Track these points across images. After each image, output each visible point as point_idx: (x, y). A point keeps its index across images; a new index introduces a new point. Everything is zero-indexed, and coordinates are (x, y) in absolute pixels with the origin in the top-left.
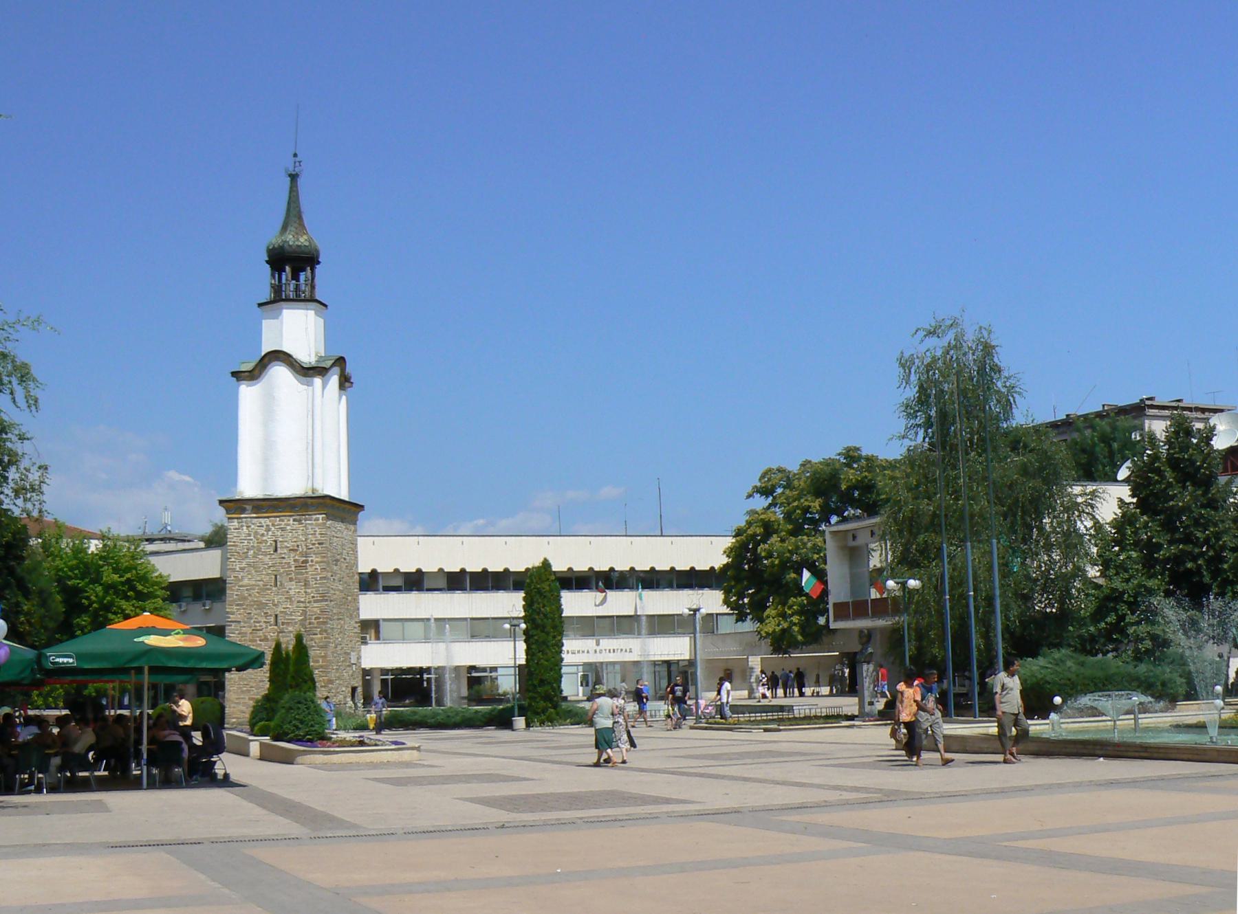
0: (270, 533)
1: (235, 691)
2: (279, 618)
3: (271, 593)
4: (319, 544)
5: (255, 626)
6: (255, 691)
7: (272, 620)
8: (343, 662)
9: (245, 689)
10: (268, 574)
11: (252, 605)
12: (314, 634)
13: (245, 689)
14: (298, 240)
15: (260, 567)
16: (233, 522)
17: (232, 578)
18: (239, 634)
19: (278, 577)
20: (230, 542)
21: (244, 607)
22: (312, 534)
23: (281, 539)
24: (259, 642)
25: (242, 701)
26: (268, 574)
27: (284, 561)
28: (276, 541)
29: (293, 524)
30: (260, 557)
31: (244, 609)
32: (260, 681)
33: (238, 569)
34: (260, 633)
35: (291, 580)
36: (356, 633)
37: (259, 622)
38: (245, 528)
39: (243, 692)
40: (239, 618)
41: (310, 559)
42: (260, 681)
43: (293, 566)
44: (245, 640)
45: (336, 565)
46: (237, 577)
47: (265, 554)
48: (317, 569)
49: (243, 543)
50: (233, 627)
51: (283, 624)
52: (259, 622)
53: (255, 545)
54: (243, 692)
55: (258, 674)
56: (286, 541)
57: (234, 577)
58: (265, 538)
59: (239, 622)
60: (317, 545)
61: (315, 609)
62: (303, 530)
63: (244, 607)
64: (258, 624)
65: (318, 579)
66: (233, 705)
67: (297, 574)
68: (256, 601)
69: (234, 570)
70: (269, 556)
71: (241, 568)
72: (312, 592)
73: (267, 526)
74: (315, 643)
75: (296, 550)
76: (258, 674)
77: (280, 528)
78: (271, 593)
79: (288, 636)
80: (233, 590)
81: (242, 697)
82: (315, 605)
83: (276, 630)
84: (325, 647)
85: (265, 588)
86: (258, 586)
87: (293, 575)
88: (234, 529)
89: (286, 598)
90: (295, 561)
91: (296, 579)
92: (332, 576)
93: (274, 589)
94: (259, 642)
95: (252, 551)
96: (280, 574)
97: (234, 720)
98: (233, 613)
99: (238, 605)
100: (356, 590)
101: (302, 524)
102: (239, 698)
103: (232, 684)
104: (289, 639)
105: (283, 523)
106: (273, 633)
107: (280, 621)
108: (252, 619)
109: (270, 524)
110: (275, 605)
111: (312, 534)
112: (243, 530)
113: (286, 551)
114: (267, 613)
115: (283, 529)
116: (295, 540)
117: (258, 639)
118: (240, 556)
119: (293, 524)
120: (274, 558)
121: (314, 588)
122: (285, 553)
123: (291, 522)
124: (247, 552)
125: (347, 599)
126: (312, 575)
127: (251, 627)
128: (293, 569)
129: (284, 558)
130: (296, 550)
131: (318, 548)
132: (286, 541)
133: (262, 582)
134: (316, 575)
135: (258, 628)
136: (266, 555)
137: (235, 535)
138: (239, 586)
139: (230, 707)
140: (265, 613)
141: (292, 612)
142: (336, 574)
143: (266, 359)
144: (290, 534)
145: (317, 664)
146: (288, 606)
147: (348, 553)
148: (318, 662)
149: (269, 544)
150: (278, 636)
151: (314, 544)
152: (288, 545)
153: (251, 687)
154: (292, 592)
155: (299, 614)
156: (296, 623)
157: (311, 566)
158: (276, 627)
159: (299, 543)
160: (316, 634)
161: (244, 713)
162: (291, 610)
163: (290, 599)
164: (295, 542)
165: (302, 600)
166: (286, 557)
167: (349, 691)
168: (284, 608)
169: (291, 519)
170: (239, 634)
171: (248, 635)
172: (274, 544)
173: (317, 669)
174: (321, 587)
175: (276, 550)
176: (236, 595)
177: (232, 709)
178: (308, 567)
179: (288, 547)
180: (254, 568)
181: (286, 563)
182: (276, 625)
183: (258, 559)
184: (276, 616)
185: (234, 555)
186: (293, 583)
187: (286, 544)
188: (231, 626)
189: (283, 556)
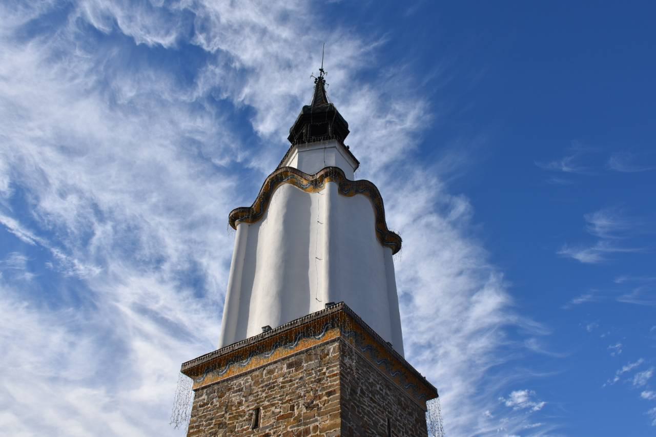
16: (202, 396)
23: (266, 403)
28: (257, 410)
41: (311, 426)
56: (273, 405)
58: (242, 408)
60: (325, 398)
62: (301, 378)
75: (291, 415)
77: (266, 386)
115: (271, 387)
123: (285, 370)
130: (291, 415)
131: (325, 402)
172: (254, 417)
187: (273, 409)
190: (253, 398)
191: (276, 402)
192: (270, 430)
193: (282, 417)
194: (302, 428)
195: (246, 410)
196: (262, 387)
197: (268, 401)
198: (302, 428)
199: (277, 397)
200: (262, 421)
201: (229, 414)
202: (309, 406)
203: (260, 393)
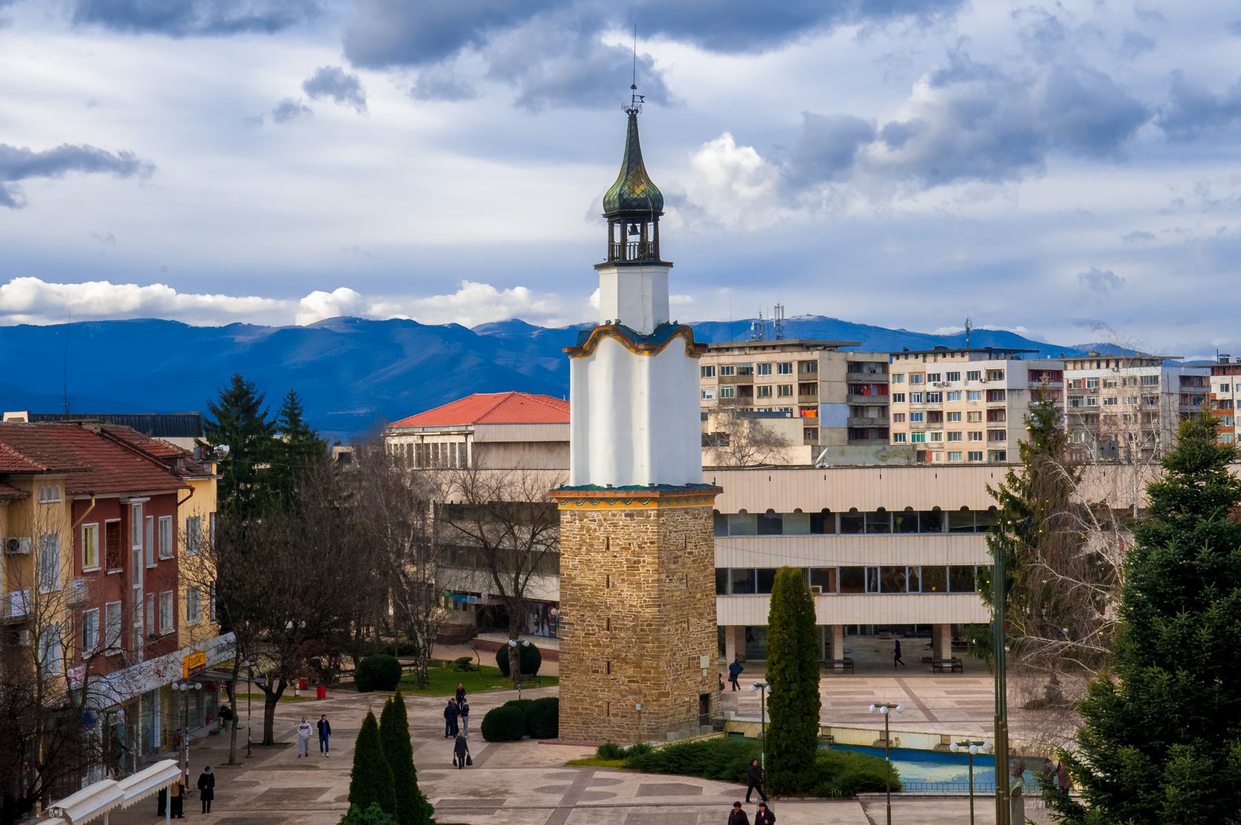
0: (602, 528)
4: (651, 543)
5: (588, 630)
7: (605, 625)
8: (685, 668)
10: (600, 574)
13: (578, 698)
14: (634, 192)
18: (572, 637)
19: (610, 577)
23: (613, 536)
24: (591, 648)
26: (600, 574)
27: (616, 560)
28: (608, 539)
30: (592, 554)
31: (577, 610)
32: (593, 690)
33: (571, 566)
34: (593, 638)
36: (710, 632)
37: (592, 626)
38: (577, 521)
39: (576, 701)
40: (572, 620)
41: (642, 559)
42: (593, 690)
43: (625, 566)
45: (675, 563)
46: (570, 575)
51: (615, 629)
52: (592, 626)
54: (576, 701)
56: (618, 538)
58: (597, 534)
59: (573, 624)
61: (647, 615)
64: (590, 628)
69: (567, 568)
71: (573, 565)
72: (644, 595)
73: (600, 520)
80: (566, 589)
81: (576, 706)
84: (657, 657)
87: (625, 577)
89: (618, 601)
90: (627, 560)
92: (667, 577)
93: (606, 590)
94: (591, 648)
95: (584, 548)
100: (710, 584)
110: (607, 608)
114: (600, 616)
116: (626, 537)
124: (580, 549)
125: (694, 597)
126: (643, 577)
127: (583, 630)
128: (625, 569)
129: (615, 557)
130: (629, 549)
131: (650, 547)
132: (618, 538)
134: (648, 577)
135: (591, 632)
136: (598, 553)
140: (598, 616)
141: (623, 617)
142: (674, 573)
145: (649, 676)
147: (696, 546)
148: (649, 672)
150: (610, 641)
151: (646, 543)
153: (585, 696)
154: (624, 594)
156: (628, 629)
157: (643, 567)
160: (648, 643)
165: (635, 603)
167: (695, 700)
169: (623, 515)
170: (572, 637)
172: (606, 542)
173: (648, 680)
174: (653, 591)
175: (608, 548)
178: (641, 569)
179: (618, 544)
180: (588, 566)
181: (618, 562)
182: (608, 630)
184: (609, 619)
185: (567, 551)
193: (624, 548)
194: (636, 558)
198: (636, 558)
202: (640, 547)
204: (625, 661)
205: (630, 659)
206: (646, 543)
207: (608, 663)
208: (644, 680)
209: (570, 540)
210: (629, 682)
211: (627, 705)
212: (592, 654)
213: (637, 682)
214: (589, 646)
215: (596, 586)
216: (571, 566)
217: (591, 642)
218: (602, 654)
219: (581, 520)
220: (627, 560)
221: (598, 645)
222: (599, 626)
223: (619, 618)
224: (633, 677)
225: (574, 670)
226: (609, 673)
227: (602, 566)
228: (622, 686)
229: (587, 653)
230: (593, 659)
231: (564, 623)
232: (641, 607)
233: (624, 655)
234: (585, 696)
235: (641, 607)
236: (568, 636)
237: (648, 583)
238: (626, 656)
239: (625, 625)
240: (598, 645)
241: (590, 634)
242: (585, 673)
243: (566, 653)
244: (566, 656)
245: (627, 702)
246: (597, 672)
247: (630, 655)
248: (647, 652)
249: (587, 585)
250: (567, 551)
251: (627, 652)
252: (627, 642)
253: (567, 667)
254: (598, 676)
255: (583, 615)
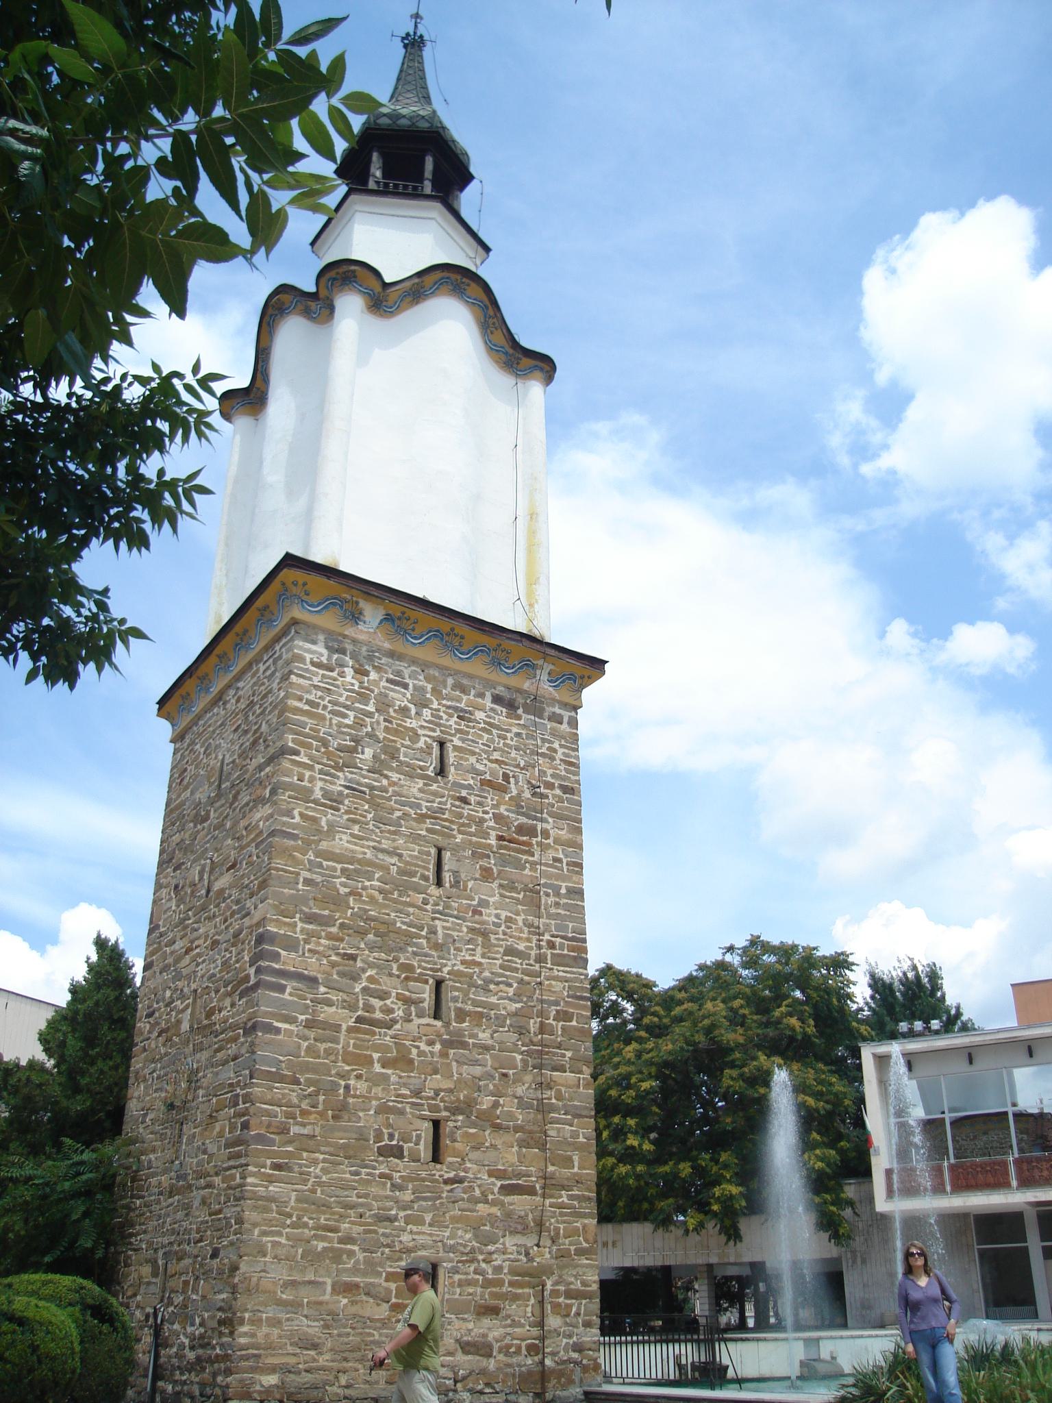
0: (427, 713)
1: (281, 1252)
2: (448, 994)
3: (425, 902)
5: (369, 1008)
6: (361, 1256)
7: (427, 994)
9: (321, 1245)
10: (415, 838)
11: (362, 933)
12: (554, 1069)
13: (321, 1245)
15: (393, 810)
17: (297, 819)
19: (447, 855)
20: (300, 699)
21: (334, 930)
22: (543, 755)
24: (377, 1068)
25: (306, 1296)
28: (442, 745)
29: (492, 710)
30: (395, 776)
31: (330, 937)
33: (318, 794)
35: (487, 874)
37: (383, 996)
38: (349, 672)
39: (313, 1257)
40: (313, 967)
43: (493, 834)
44: (328, 1052)
46: (315, 820)
47: (411, 773)
48: (559, 860)
49: (345, 716)
50: (286, 996)
51: (461, 1015)
52: (383, 996)
53: (381, 735)
54: (313, 1257)
55: (374, 1190)
56: (473, 753)
57: (301, 814)
59: (314, 980)
60: (558, 792)
62: (518, 735)
63: (334, 930)
64: (376, 1003)
65: (563, 891)
66: (269, 1313)
67: (504, 861)
68: (374, 919)
69: (304, 795)
70: (421, 783)
71: (326, 794)
74: (559, 1097)
76: (374, 1190)
77: (456, 709)
78: (425, 902)
79: (476, 1063)
80: (297, 862)
82: (559, 971)
83: (439, 1035)
85: (401, 883)
86: (386, 869)
88: (313, 663)
89: (471, 930)
90: (498, 818)
91: (500, 872)
93: (433, 890)
96: (456, 849)
97: (271, 1380)
98: (291, 945)
99: (309, 918)
101: (519, 718)
102: (293, 1283)
103: (269, 1222)
104: (478, 1071)
105: (465, 698)
106: (431, 1043)
107: (450, 1007)
108: (355, 978)
109: (429, 687)
110: (437, 947)
111: (543, 755)
112: (342, 675)
113: (471, 782)
116: (496, 756)
117: (376, 1056)
118: (329, 755)
119: (492, 710)
120: (435, 794)
121: (549, 916)
122: (469, 787)
124: (353, 750)
127: (352, 1007)
129: (464, 801)
132: (473, 753)
133: (394, 860)
134: (558, 877)
135: (378, 1015)
136: (411, 776)
137: (316, 681)
138: (318, 854)
139: (256, 1322)
141: (487, 981)
143: (430, 279)
144: (486, 736)
145: (566, 1172)
146: (478, 958)
148: (568, 1162)
149: (421, 744)
151: (550, 786)
152: (480, 767)
153: (348, 1239)
154: (489, 915)
155: (511, 991)
156: (500, 1020)
158: (439, 1023)
159: (510, 770)
161: (315, 1346)
162: (487, 974)
163: (485, 934)
164: (497, 761)
166: (472, 799)
168: (463, 962)
170: (309, 1025)
171: (342, 1036)
173: (563, 1187)
175: (442, 771)
176: (307, 882)
177: (265, 1329)
179: (478, 773)
180: (375, 806)
181: (470, 817)
183: (385, 782)
184: (439, 984)
185: (309, 746)
186: (495, 885)
187: (473, 760)
188: (282, 989)
189: (464, 793)
190: (429, 718)
191: (477, 750)
192: (470, 794)
194: (523, 820)
195: (420, 732)
196: (449, 707)
197: (460, 739)
198: (523, 820)
199: (478, 743)
200: (452, 769)
201: (385, 720)
203: (445, 717)
204: (490, 1121)
205: (511, 1116)
206: (550, 786)
207: (436, 1124)
208: (550, 1185)
209: (323, 718)
210: (508, 1190)
211: (498, 1269)
212: (377, 1091)
213: (530, 1191)
214: (369, 1061)
215: (402, 872)
216: (318, 794)
217: (377, 1048)
218: (417, 1093)
219: (360, 672)
220: (498, 818)
221: (402, 1061)
222: (407, 1001)
223: (473, 985)
224: (519, 1175)
225: (307, 1143)
226: (436, 1158)
227: (422, 818)
228: (480, 1206)
229: (361, 1087)
230: (383, 1109)
231: (282, 974)
232: (540, 959)
233: (486, 1102)
234: (348, 1239)
235: (540, 959)
236: (292, 1020)
237: (558, 894)
238: (496, 1105)
239: (492, 1007)
240: (402, 1061)
241: (373, 1023)
242: (350, 1153)
243: (282, 1079)
244: (280, 1089)
245: (498, 1260)
246: (398, 1152)
247: (508, 1105)
248: (559, 1097)
249: (370, 863)
250: (308, 746)
251: (498, 1094)
252: (501, 1064)
253: (283, 1130)
254: (401, 1168)
255: (353, 958)
